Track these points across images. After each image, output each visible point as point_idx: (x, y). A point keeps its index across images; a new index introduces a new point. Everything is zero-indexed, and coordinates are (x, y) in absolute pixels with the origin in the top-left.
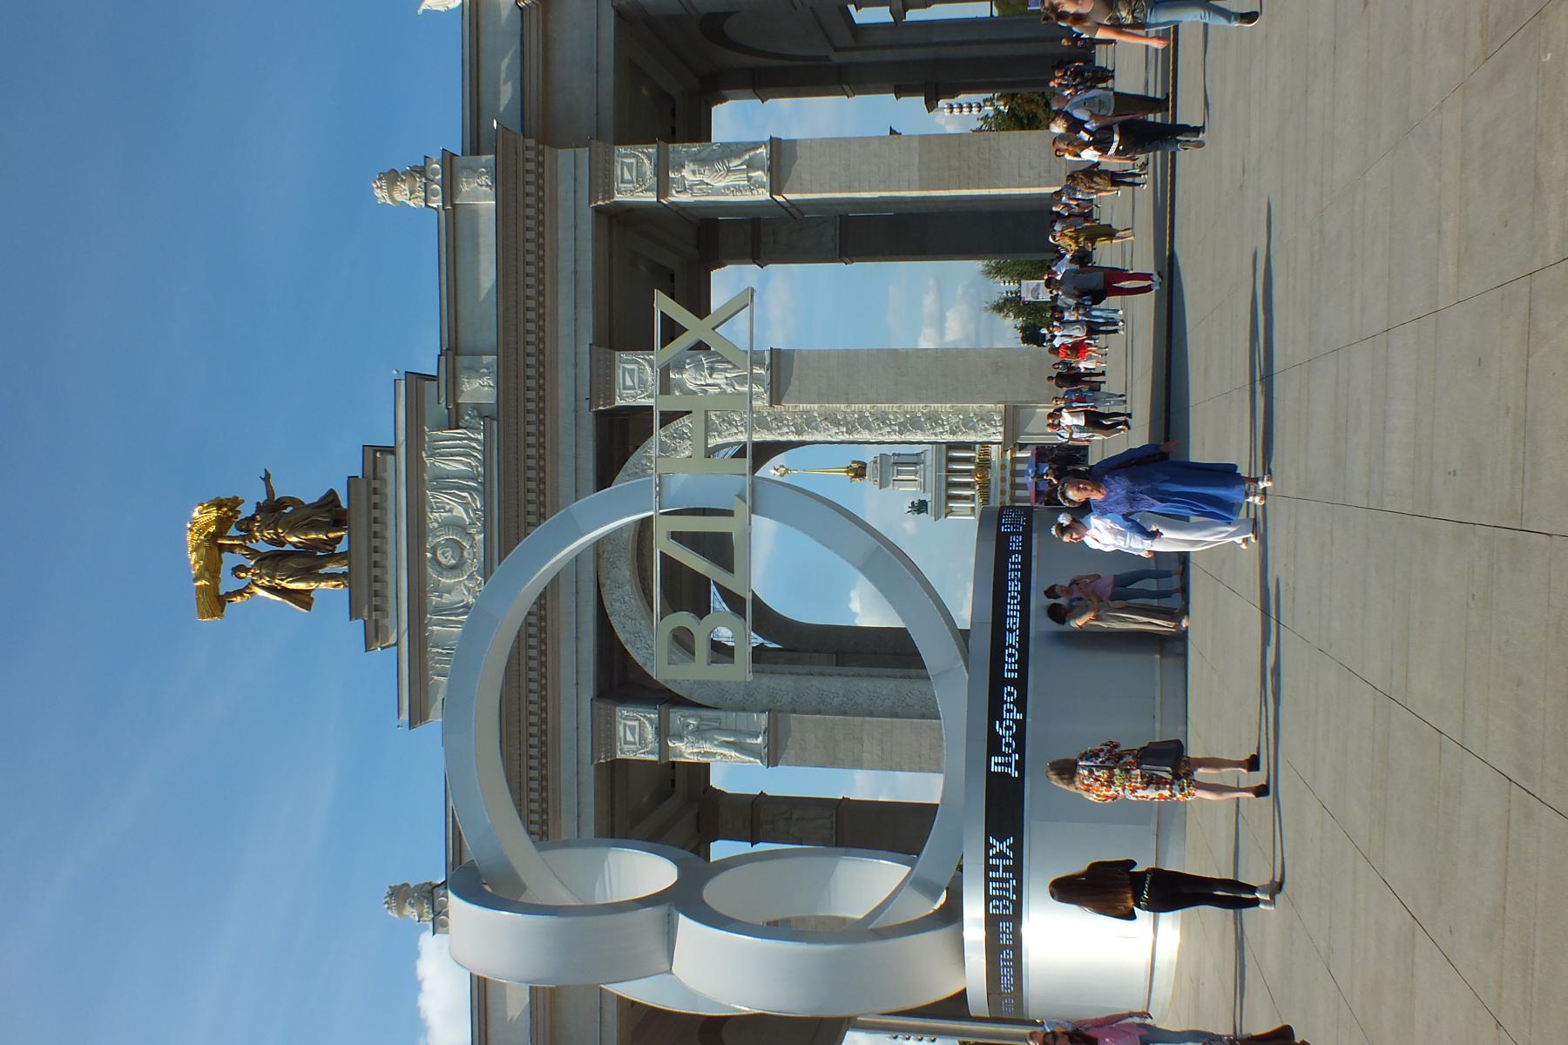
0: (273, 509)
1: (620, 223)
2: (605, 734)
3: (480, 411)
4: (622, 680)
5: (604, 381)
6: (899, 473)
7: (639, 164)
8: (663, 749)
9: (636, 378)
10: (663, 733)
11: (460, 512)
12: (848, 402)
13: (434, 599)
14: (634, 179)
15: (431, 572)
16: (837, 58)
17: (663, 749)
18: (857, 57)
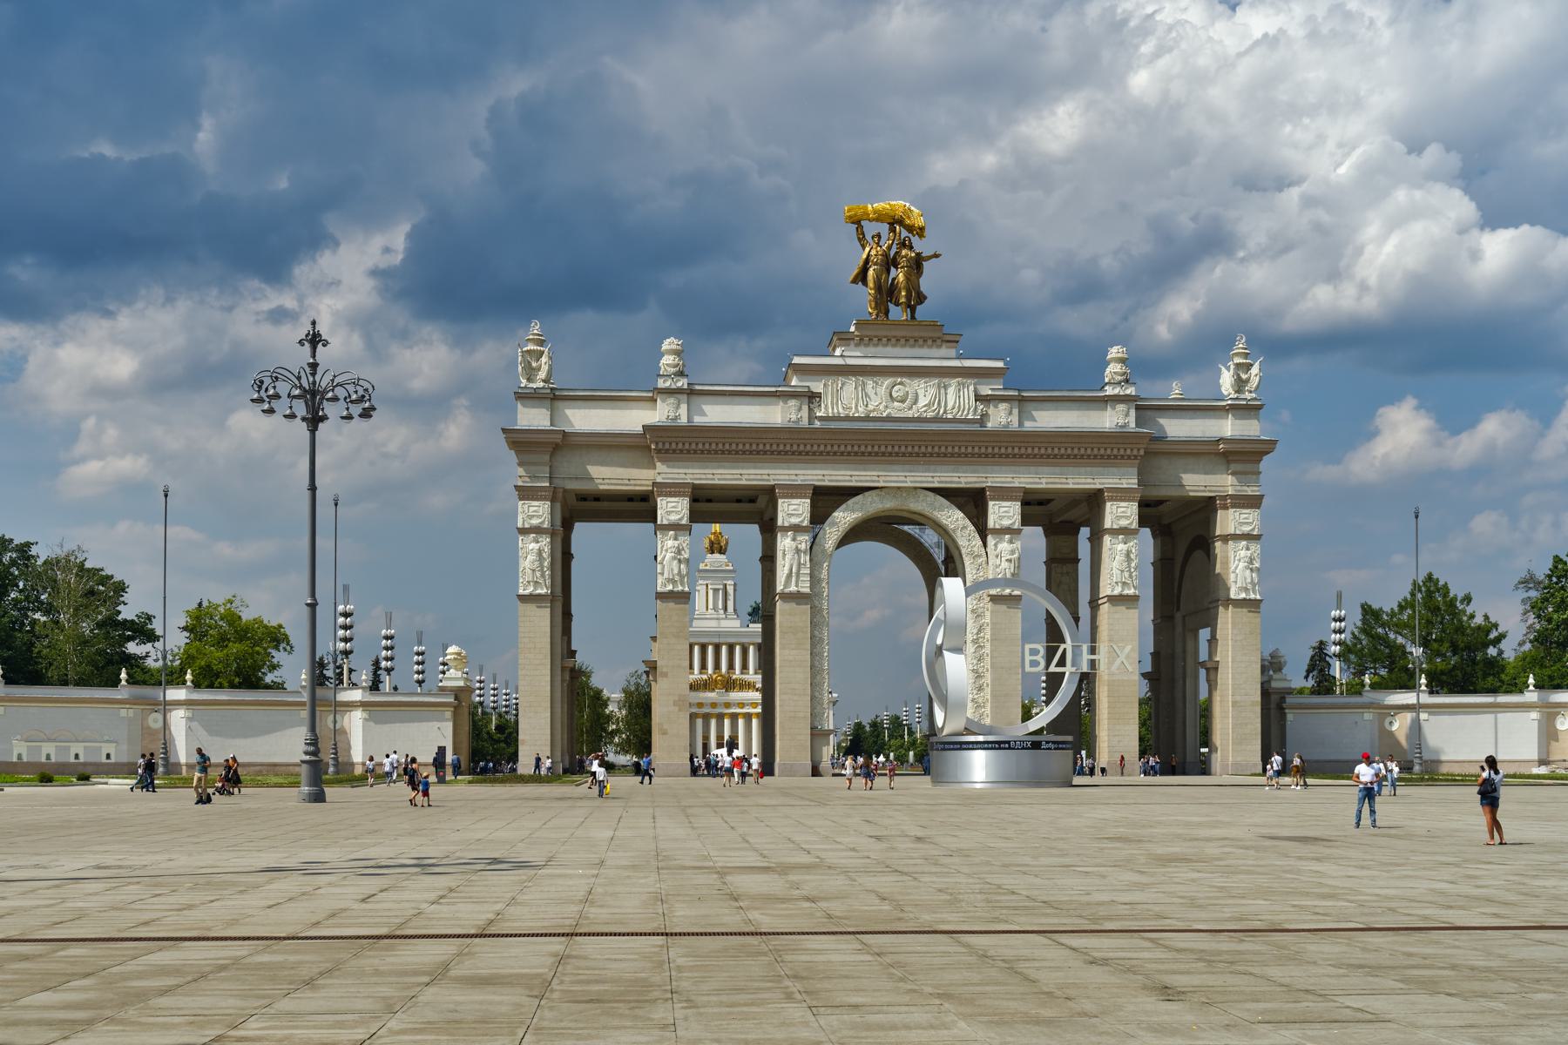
0: (917, 264)
1: (1094, 501)
2: (794, 491)
3: (985, 416)
4: (825, 500)
5: (1004, 494)
6: (716, 591)
7: (1127, 518)
8: (785, 529)
9: (1003, 513)
10: (796, 529)
11: (922, 402)
12: (993, 639)
13: (870, 383)
14: (1121, 513)
15: (888, 381)
16: (1178, 616)
17: (785, 529)
18: (1179, 629)
